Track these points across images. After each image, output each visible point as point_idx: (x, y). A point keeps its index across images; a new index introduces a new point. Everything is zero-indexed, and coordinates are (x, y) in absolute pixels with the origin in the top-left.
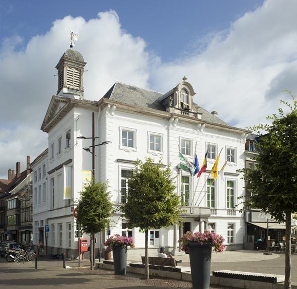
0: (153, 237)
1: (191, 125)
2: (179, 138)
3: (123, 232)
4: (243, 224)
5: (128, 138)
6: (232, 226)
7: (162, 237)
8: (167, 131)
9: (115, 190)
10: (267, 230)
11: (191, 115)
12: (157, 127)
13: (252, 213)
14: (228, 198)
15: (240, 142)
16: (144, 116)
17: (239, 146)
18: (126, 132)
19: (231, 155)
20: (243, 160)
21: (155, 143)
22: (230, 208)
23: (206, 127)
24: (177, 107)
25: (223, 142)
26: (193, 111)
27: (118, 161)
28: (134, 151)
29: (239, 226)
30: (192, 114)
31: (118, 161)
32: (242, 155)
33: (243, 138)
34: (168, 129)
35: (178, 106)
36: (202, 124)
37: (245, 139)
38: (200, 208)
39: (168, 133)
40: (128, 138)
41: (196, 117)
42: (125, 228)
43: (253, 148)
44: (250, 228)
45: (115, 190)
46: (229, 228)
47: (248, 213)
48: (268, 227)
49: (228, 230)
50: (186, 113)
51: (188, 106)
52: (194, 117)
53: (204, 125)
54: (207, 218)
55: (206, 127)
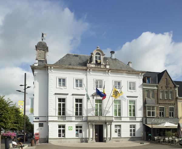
0: (78, 132)
1: (102, 72)
2: (94, 79)
3: (59, 130)
4: (142, 125)
5: (62, 82)
6: (134, 126)
7: (83, 132)
8: (86, 76)
9: (54, 109)
10: (152, 129)
11: (102, 67)
12: (80, 75)
13: (147, 118)
14: (130, 111)
15: (139, 78)
16: (71, 70)
17: (138, 81)
18: (61, 79)
19: (132, 86)
20: (141, 89)
21: (79, 83)
22: (132, 116)
23: (111, 72)
24: (92, 63)
25: (125, 79)
26: (103, 64)
27: (56, 94)
28: (82, 89)
29: (138, 126)
30: (103, 66)
31: (56, 94)
32: (140, 86)
33: (141, 76)
34: (86, 75)
35: (94, 62)
36: (108, 71)
37: (142, 76)
38: (106, 117)
39: (87, 77)
40: (62, 82)
41: (106, 67)
42: (61, 128)
43: (150, 81)
44: (147, 129)
45: (54, 109)
46: (130, 127)
47: (144, 119)
48: (152, 127)
49: (131, 129)
50: (99, 66)
51: (101, 62)
52: (104, 67)
53: (110, 71)
54: (111, 122)
55: (111, 72)
